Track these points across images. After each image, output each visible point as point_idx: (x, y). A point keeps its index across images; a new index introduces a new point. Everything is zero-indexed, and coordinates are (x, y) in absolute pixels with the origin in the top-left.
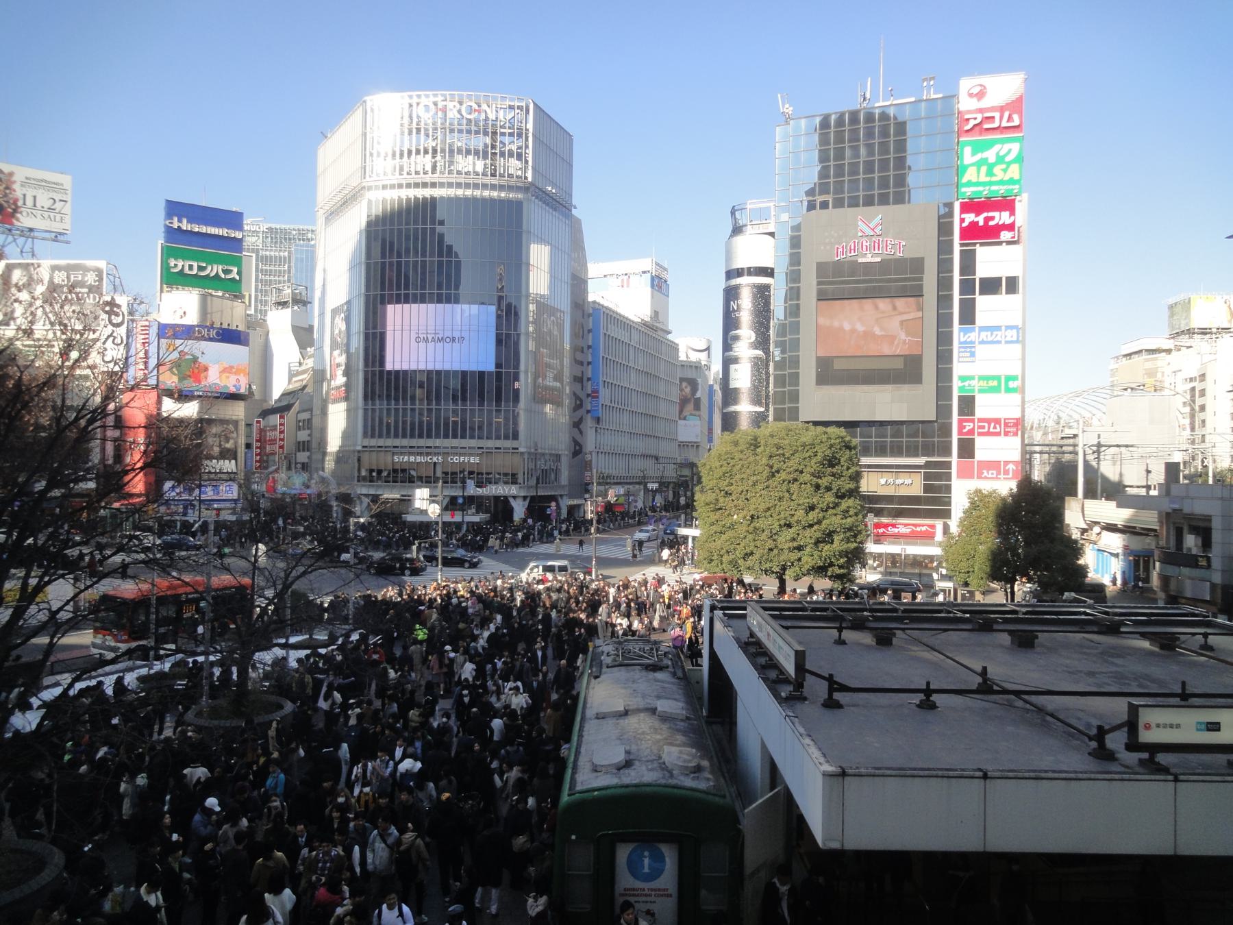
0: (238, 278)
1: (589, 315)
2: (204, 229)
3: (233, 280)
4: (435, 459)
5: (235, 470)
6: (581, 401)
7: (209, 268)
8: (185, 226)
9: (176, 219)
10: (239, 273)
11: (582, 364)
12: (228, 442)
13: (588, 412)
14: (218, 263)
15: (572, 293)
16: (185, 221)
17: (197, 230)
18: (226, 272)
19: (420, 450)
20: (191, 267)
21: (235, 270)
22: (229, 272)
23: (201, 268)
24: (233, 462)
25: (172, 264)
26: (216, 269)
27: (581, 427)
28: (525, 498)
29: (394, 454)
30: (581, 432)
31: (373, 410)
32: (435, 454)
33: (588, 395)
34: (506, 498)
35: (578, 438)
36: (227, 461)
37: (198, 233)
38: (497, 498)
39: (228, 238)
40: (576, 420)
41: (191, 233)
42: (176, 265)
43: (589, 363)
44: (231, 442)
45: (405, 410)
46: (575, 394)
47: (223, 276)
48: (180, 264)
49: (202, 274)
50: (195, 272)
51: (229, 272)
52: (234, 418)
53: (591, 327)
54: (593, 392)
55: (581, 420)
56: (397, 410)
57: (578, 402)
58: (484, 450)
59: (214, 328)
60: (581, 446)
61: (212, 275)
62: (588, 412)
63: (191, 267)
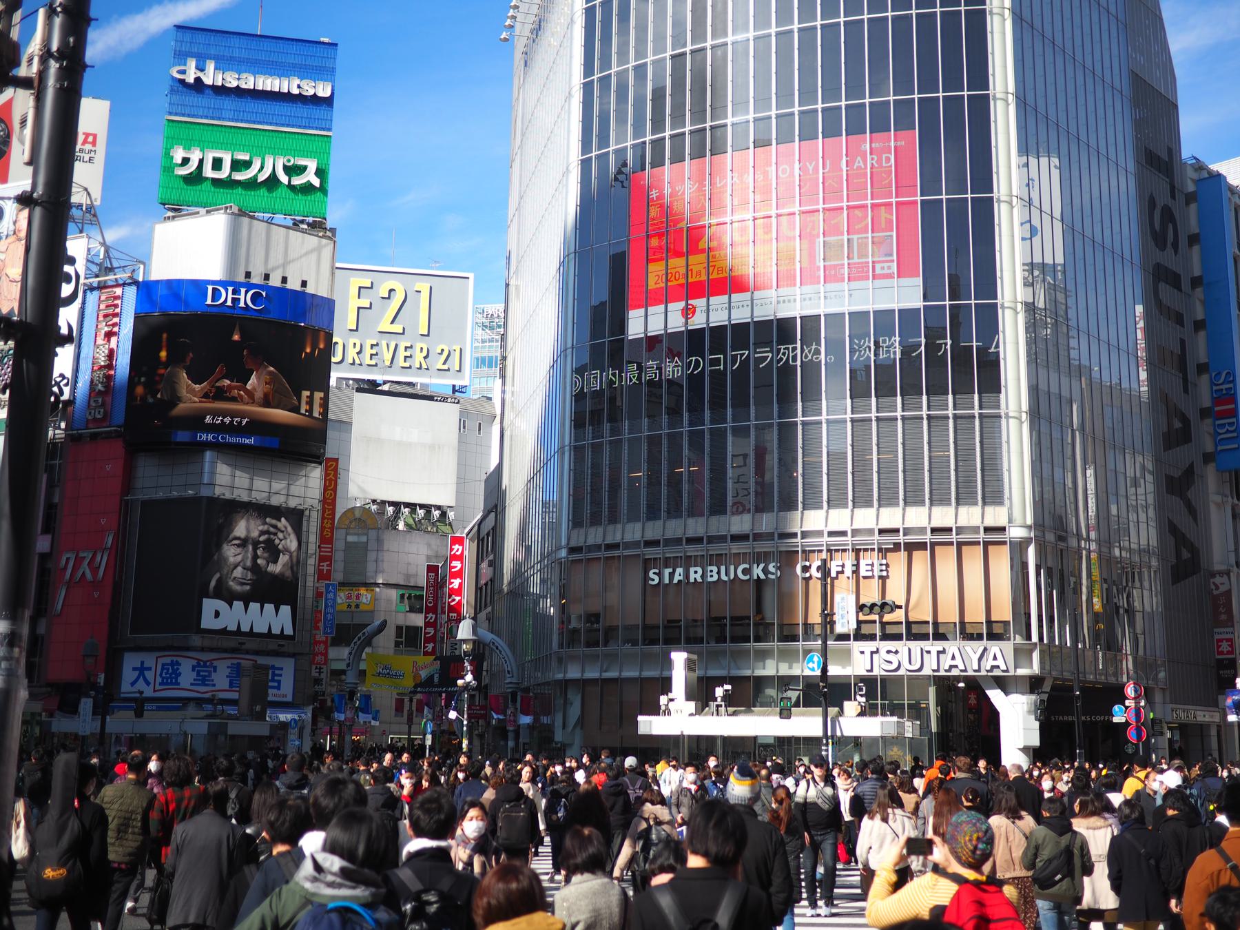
0: (316, 182)
1: (1190, 198)
2: (248, 82)
3: (308, 189)
4: (758, 571)
5: (289, 631)
6: (1185, 420)
7: (256, 165)
8: (210, 77)
9: (192, 64)
10: (320, 173)
11: (1179, 319)
12: (275, 561)
13: (1208, 458)
14: (275, 152)
15: (1138, 125)
16: (211, 66)
17: (234, 84)
18: (289, 170)
19: (715, 549)
20: (217, 164)
21: (312, 166)
22: (302, 170)
23: (237, 165)
24: (286, 610)
25: (178, 155)
26: (273, 164)
27: (1190, 494)
28: (1033, 684)
29: (647, 564)
30: (1192, 511)
31: (597, 448)
32: (758, 558)
33: (1205, 413)
34: (975, 686)
35: (1183, 522)
36: (269, 607)
37: (238, 92)
38: (945, 685)
39: (301, 99)
40: (1176, 474)
41: (221, 91)
42: (186, 161)
43: (1199, 325)
44: (283, 559)
45: (674, 439)
46: (1166, 399)
47: (284, 179)
48: (195, 157)
49: (238, 176)
50: (224, 174)
51: (302, 170)
52: (293, 503)
53: (1194, 228)
54: (1217, 401)
55: (1189, 473)
56: (654, 442)
57: (1177, 424)
58: (901, 538)
59: (249, 286)
60: (1194, 551)
61: (261, 178)
62: (1208, 458)
63: (217, 164)
